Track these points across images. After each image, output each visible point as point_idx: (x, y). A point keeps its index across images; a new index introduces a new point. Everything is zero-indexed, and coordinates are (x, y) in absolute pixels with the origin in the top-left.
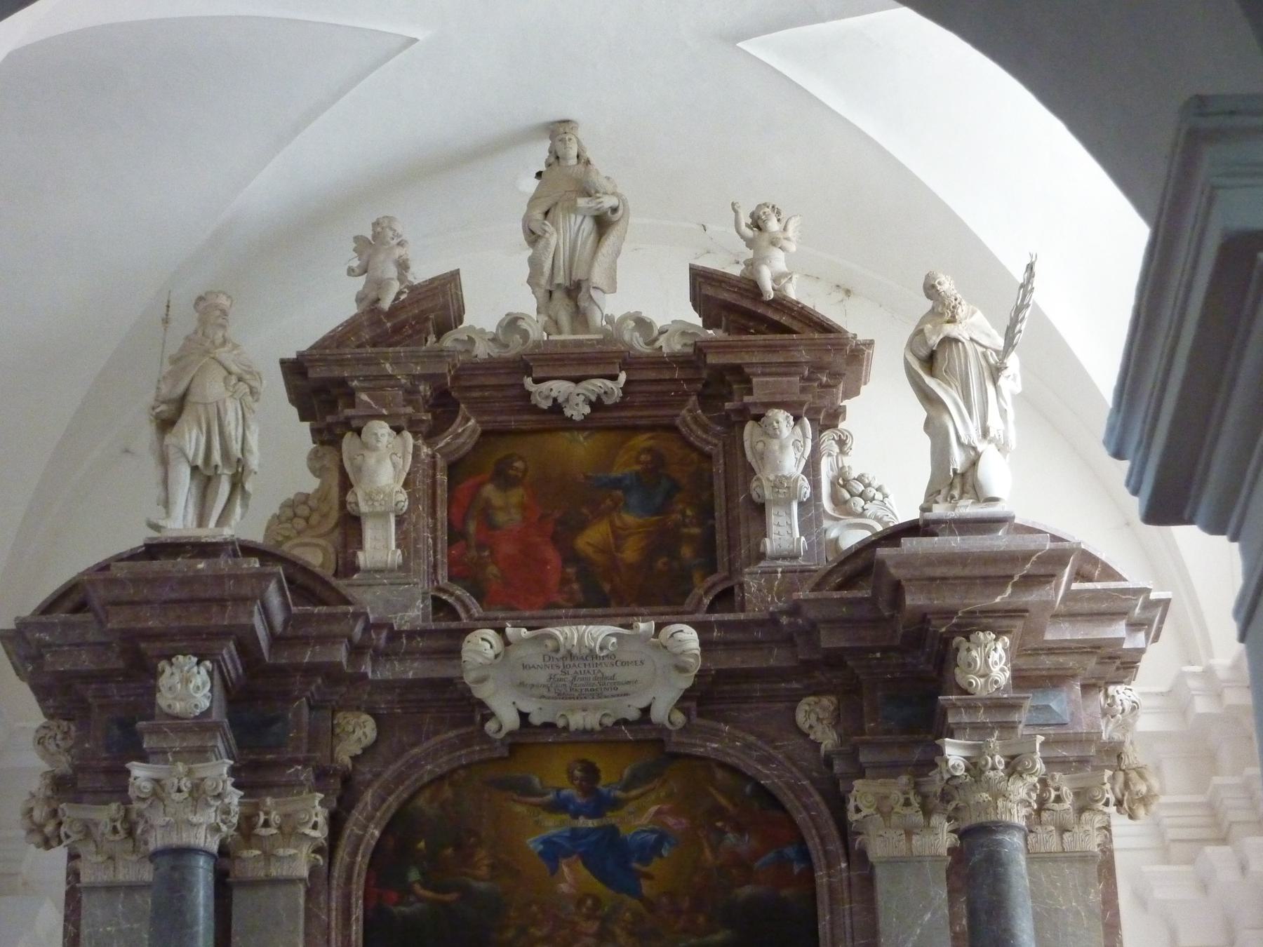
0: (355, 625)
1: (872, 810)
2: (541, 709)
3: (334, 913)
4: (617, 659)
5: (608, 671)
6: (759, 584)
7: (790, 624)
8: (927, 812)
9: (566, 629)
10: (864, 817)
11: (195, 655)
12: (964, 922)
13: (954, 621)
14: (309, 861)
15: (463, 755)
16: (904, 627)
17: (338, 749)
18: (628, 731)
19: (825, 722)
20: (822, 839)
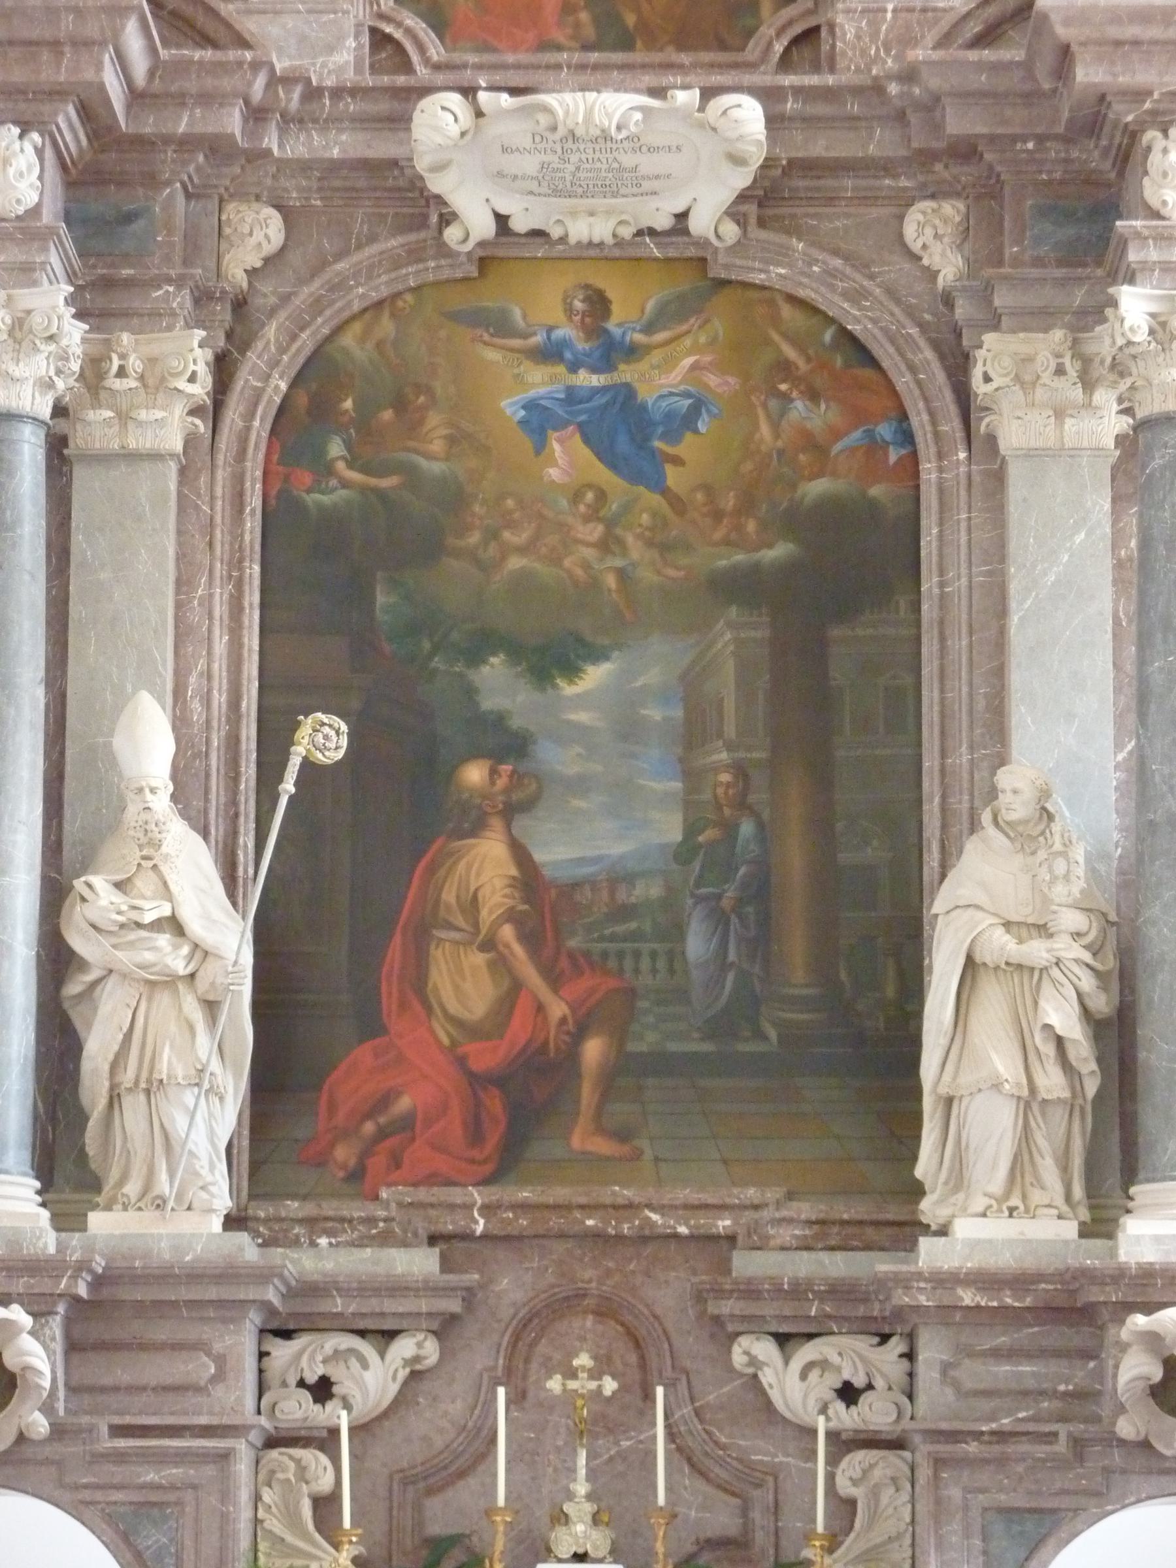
0: (255, 79)
1: (1007, 380)
2: (527, 209)
3: (219, 503)
4: (642, 142)
5: (628, 160)
6: (859, 28)
7: (901, 95)
8: (1088, 383)
9: (568, 97)
10: (997, 390)
11: (16, 123)
12: (1133, 543)
13: (1148, 105)
14: (185, 427)
15: (411, 275)
16: (1071, 110)
17: (227, 257)
18: (655, 244)
19: (946, 240)
20: (932, 414)
